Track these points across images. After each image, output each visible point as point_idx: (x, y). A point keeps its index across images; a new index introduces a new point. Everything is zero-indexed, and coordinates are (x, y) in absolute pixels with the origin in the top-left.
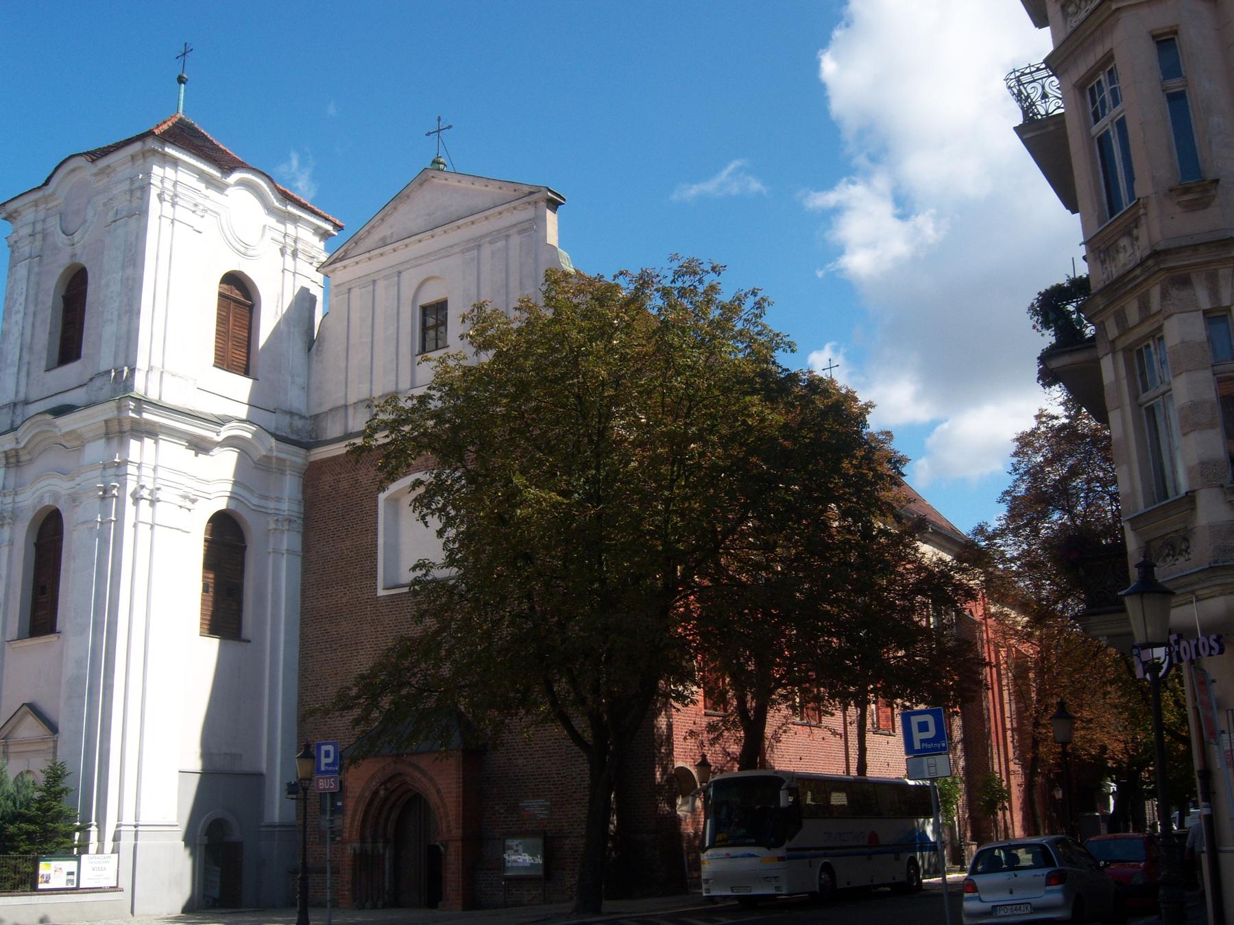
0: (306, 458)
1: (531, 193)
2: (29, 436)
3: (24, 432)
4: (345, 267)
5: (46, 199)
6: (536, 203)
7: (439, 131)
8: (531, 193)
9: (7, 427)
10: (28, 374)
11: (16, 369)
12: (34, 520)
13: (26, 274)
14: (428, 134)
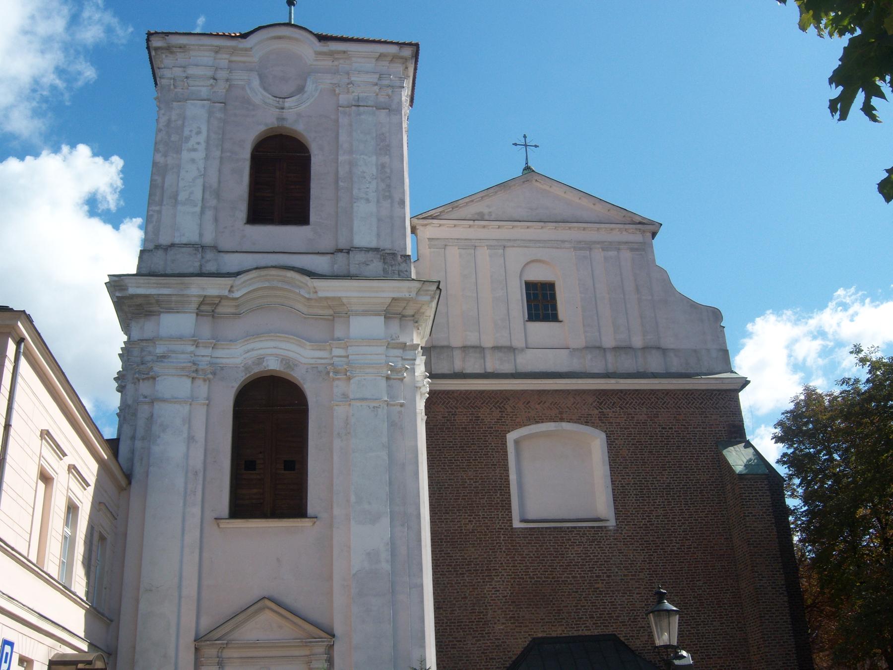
1: (640, 223)
2: (251, 288)
3: (244, 282)
4: (440, 225)
5: (234, 51)
6: (644, 231)
8: (640, 223)
9: (197, 271)
10: (216, 220)
11: (198, 209)
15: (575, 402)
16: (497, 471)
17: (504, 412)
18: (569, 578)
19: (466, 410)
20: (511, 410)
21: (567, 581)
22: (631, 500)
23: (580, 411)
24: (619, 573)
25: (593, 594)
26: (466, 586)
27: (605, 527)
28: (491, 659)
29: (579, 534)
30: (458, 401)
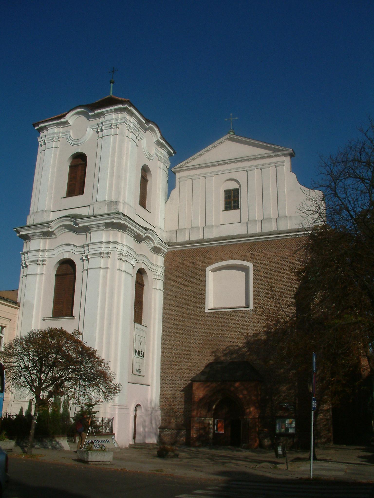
15: (239, 250)
16: (201, 286)
17: (205, 257)
18: (229, 335)
19: (189, 258)
20: (209, 257)
21: (228, 336)
22: (262, 297)
23: (241, 253)
25: (239, 342)
26: (183, 339)
27: (248, 310)
28: (191, 371)
29: (235, 314)
30: (186, 254)
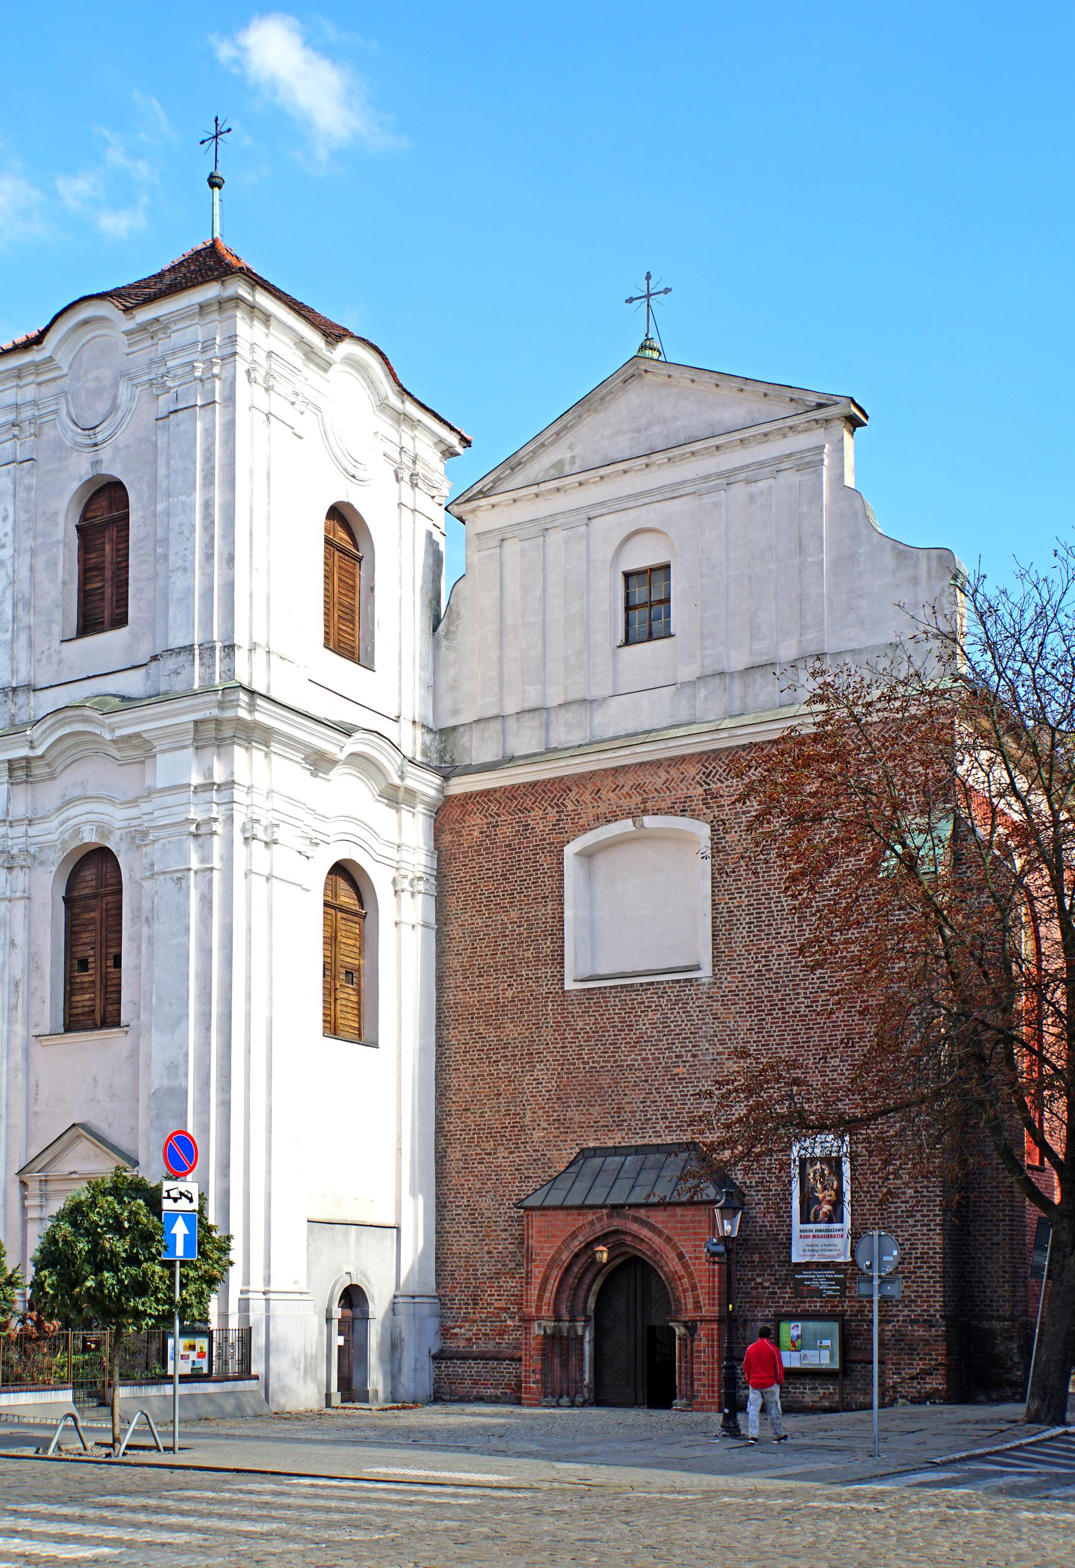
0: (441, 790)
7: (649, 296)
10: (30, 644)
12: (65, 861)
13: (11, 487)
14: (630, 300)
20: (574, 808)
23: (674, 792)
24: (711, 1051)
30: (500, 803)
